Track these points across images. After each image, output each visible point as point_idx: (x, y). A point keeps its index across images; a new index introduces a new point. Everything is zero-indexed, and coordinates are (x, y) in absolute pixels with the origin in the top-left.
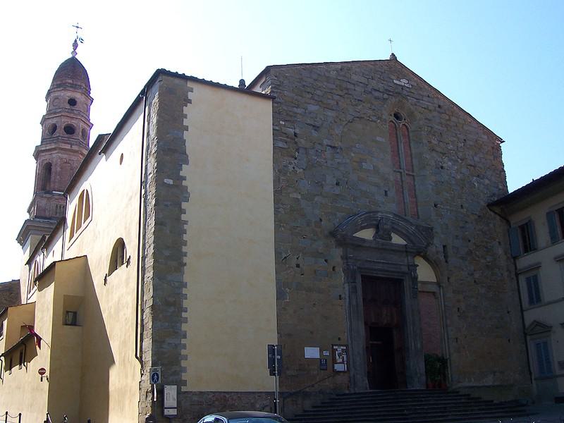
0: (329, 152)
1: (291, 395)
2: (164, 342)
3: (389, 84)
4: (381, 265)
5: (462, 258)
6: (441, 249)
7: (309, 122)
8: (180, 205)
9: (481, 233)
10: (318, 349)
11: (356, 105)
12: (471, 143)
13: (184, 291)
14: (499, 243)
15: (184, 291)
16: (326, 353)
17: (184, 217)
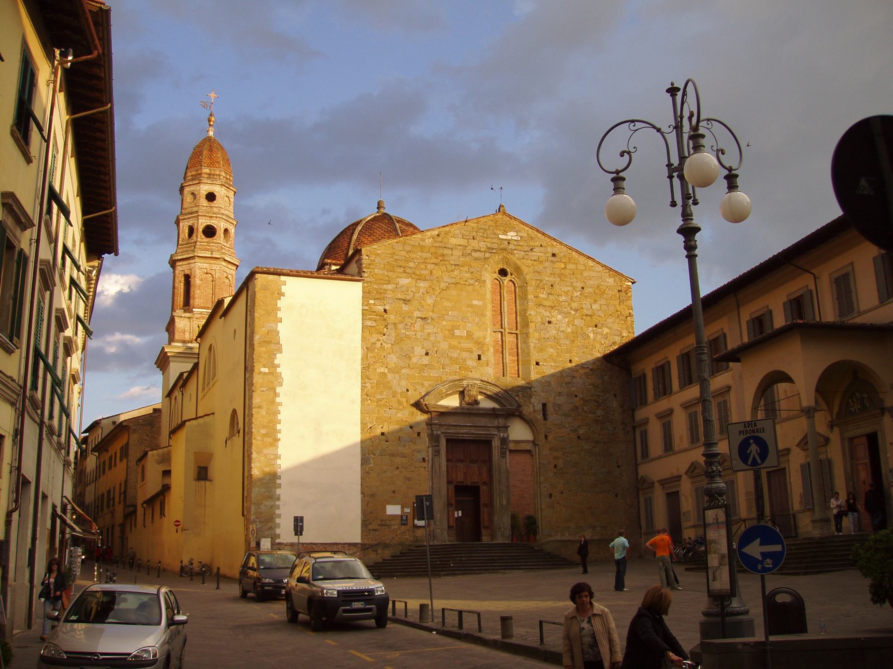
0: (419, 323)
1: (371, 546)
2: (261, 503)
3: (494, 241)
5: (566, 415)
6: (539, 407)
7: (399, 296)
8: (275, 389)
11: (452, 271)
12: (590, 290)
14: (615, 396)
17: (278, 400)
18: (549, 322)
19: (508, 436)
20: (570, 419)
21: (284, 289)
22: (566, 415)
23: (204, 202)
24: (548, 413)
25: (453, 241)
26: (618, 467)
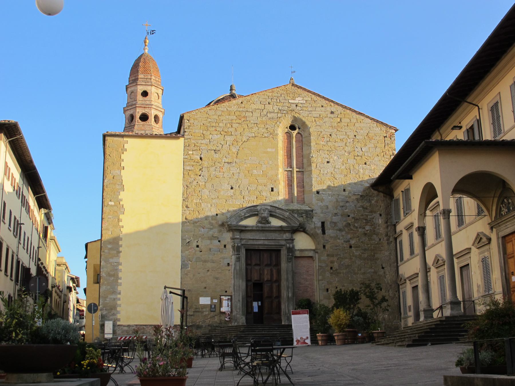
2: (107, 297)
4: (262, 241)
5: (340, 230)
6: (319, 225)
9: (361, 209)
10: (209, 299)
13: (120, 267)
14: (381, 215)
15: (120, 267)
16: (215, 301)
17: (121, 224)
18: (328, 162)
19: (293, 246)
20: (343, 233)
21: (126, 146)
22: (340, 230)
23: (140, 97)
24: (326, 228)
25: (254, 107)
26: (383, 268)
